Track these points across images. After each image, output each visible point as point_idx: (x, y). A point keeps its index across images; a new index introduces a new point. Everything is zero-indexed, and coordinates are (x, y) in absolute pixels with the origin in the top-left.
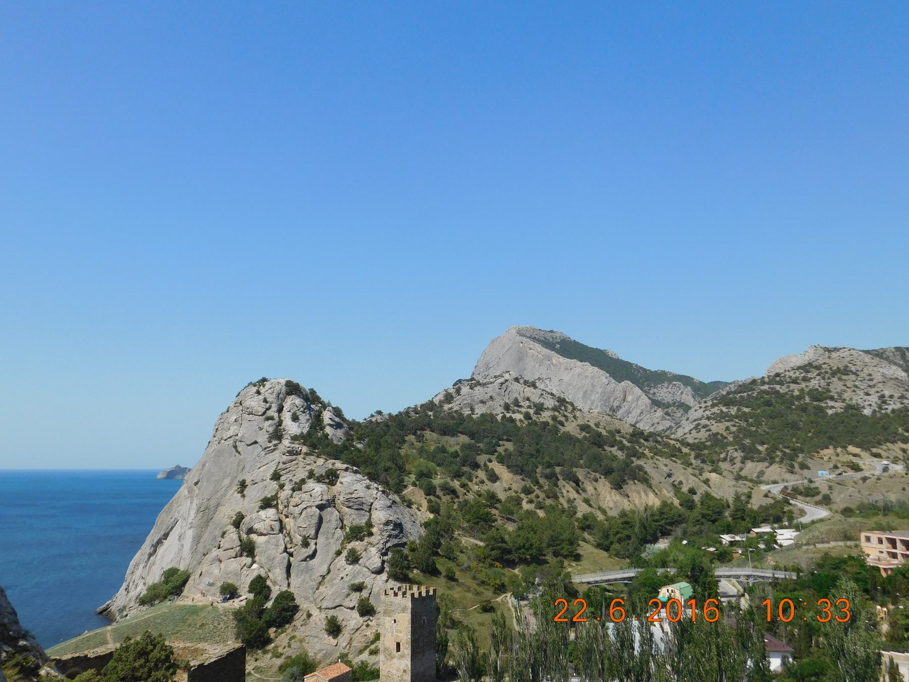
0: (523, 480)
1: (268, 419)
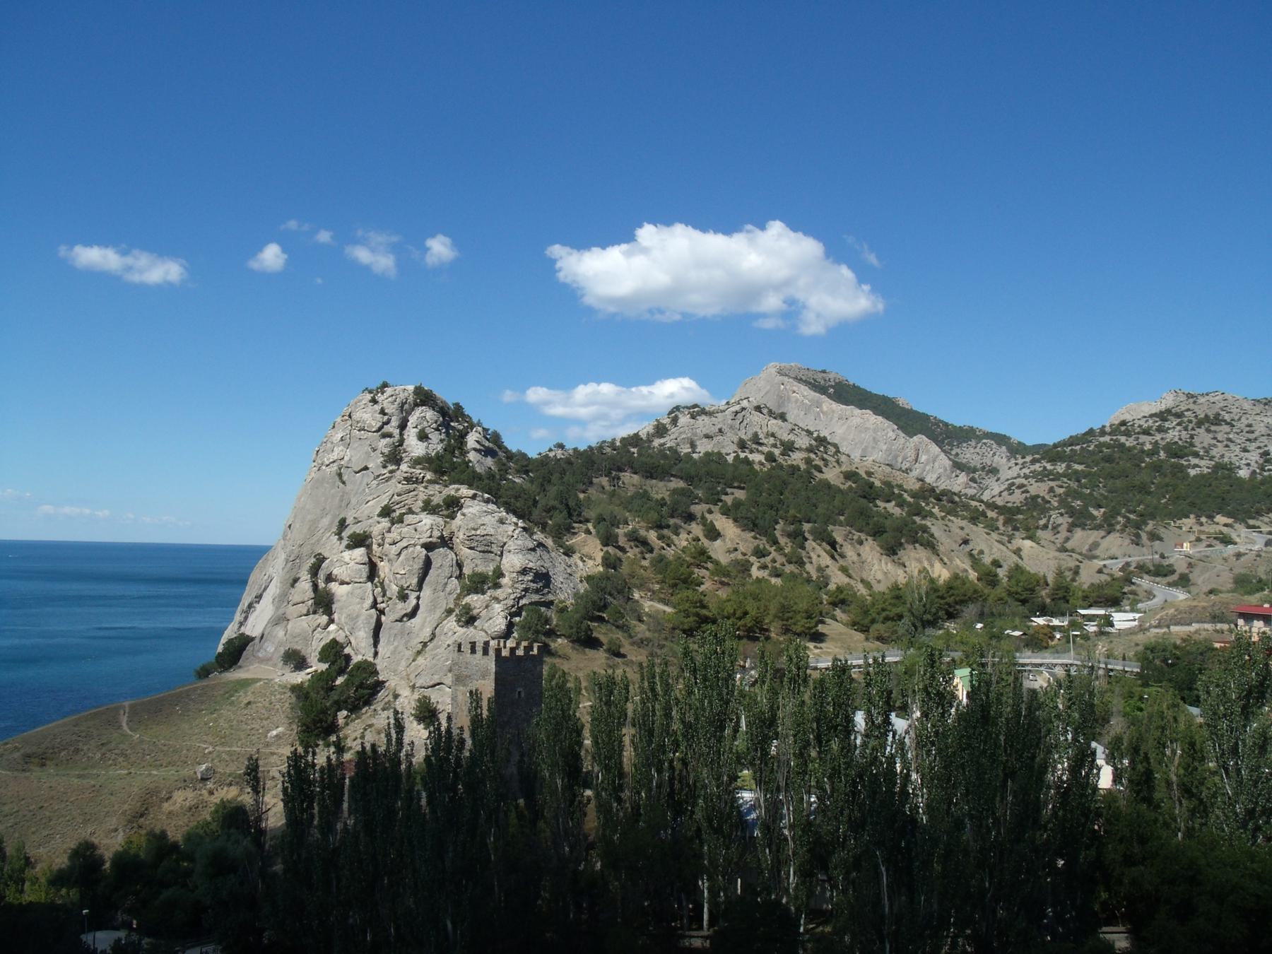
0: (755, 538)
1: (385, 436)
